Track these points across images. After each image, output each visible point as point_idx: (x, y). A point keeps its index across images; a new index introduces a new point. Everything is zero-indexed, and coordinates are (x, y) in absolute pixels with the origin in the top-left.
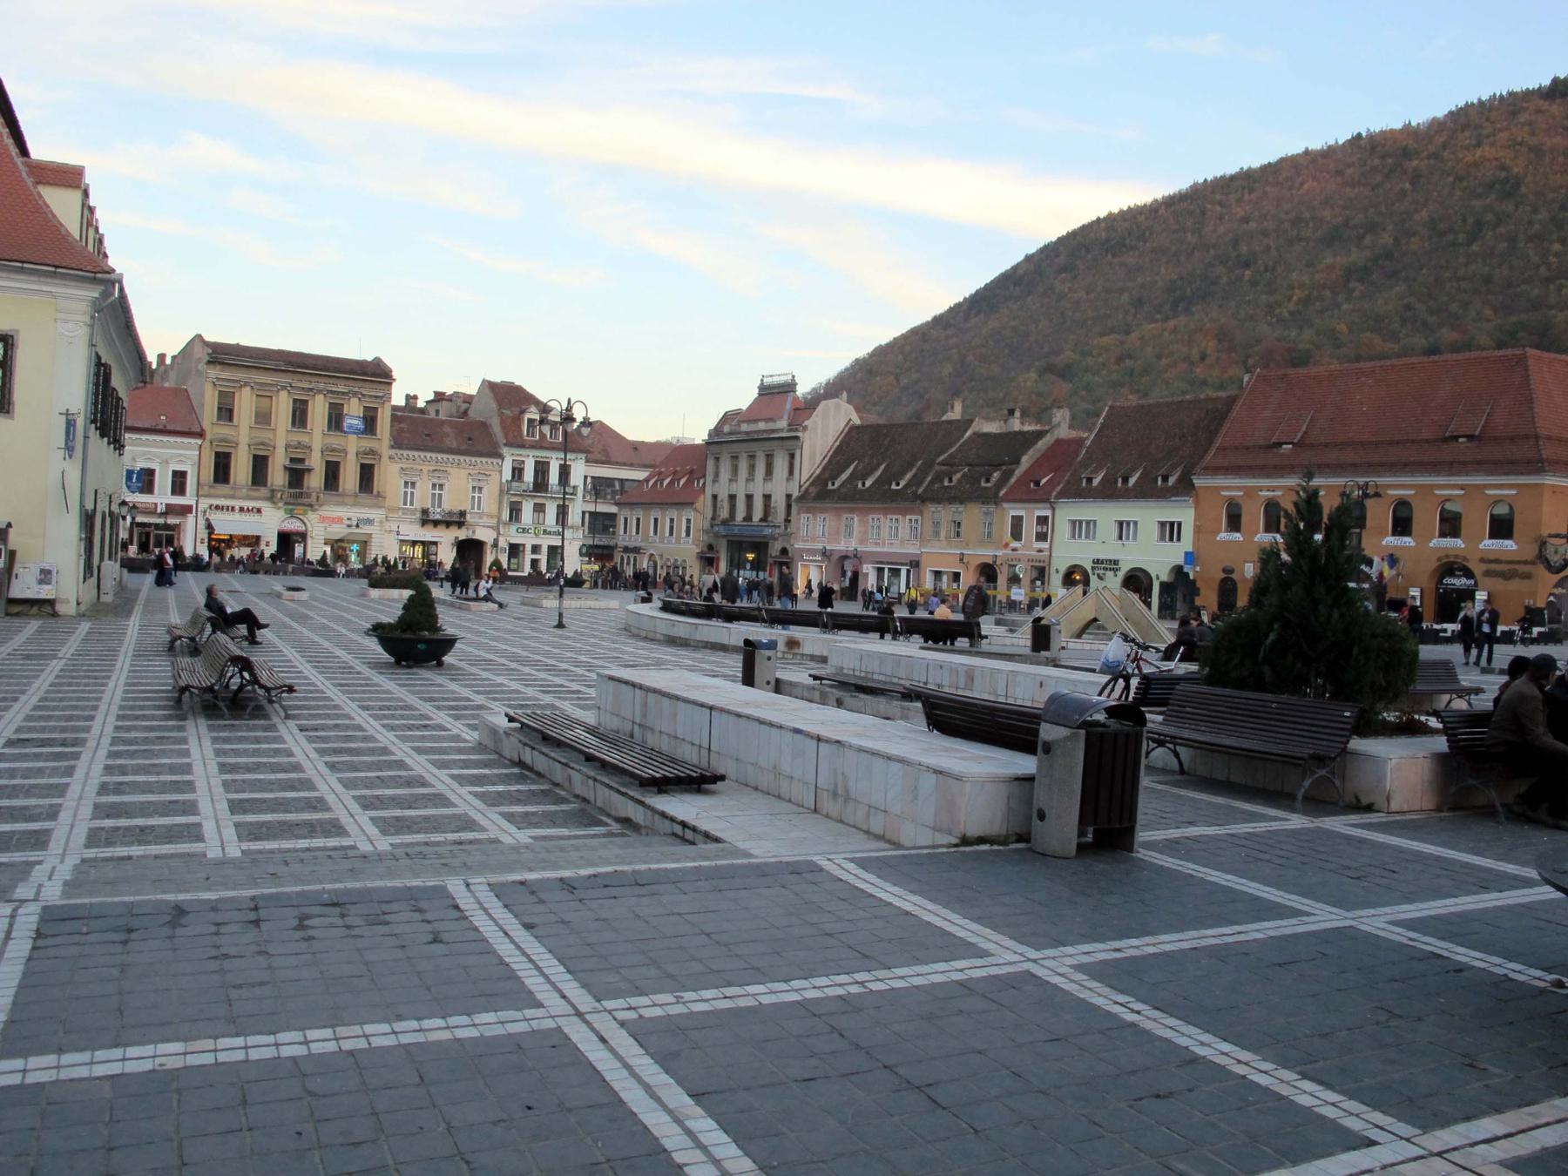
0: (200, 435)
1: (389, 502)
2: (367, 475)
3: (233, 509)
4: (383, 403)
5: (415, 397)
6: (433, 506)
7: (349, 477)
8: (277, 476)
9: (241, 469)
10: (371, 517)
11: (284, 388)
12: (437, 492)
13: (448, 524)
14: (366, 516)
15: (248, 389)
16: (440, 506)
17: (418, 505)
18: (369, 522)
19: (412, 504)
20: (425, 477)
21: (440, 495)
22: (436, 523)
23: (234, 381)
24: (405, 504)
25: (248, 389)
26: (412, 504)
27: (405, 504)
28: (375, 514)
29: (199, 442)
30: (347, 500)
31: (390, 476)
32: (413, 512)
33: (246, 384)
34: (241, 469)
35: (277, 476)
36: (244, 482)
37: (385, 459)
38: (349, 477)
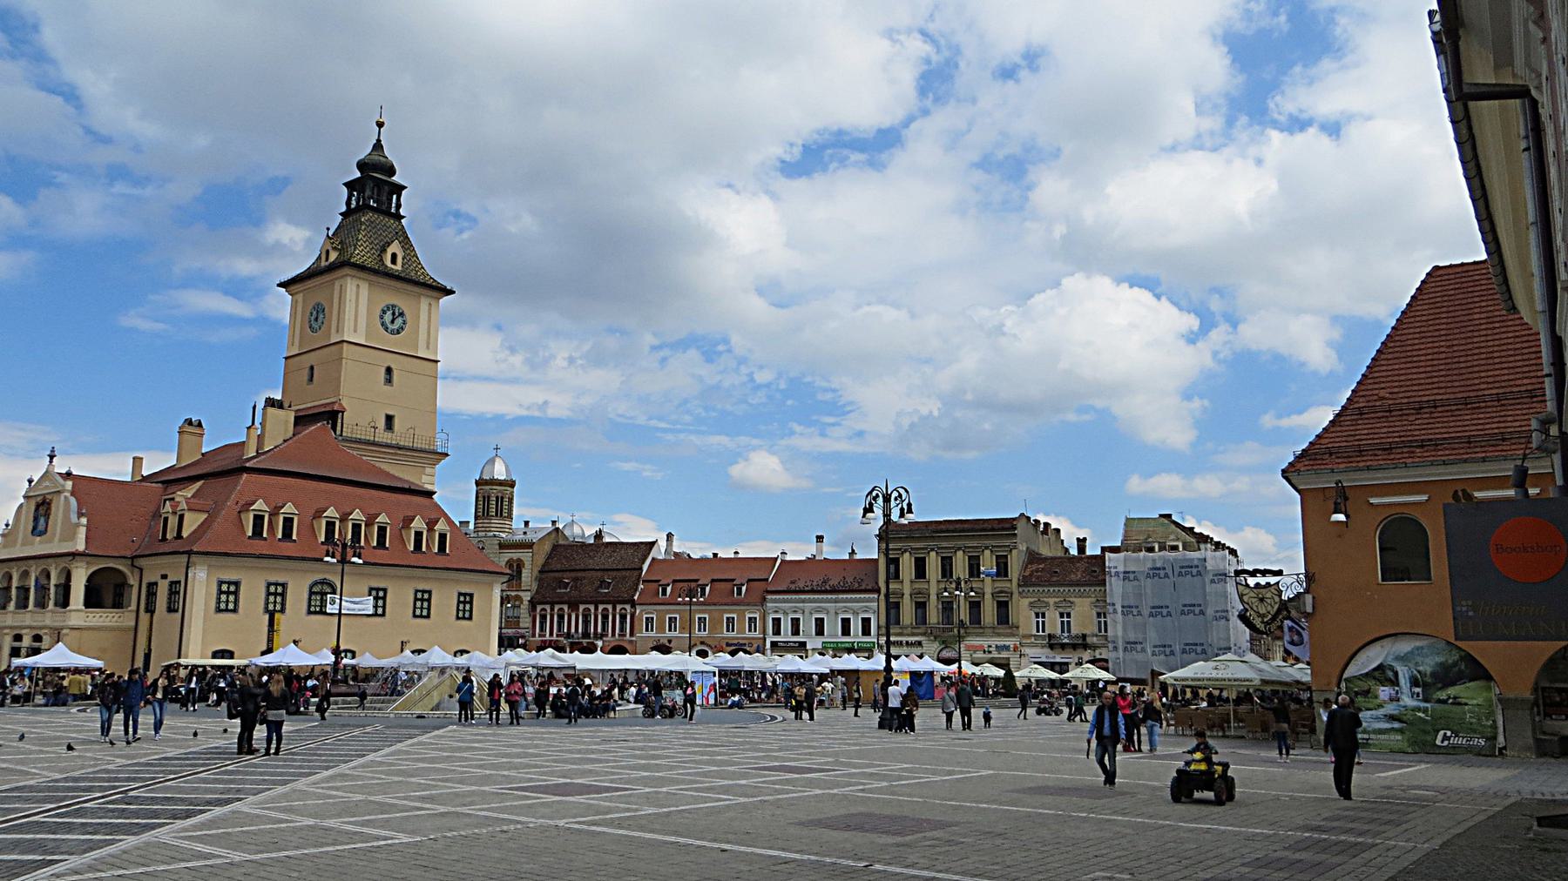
0: (878, 591)
1: (1021, 631)
2: (1003, 607)
3: (901, 642)
4: (1011, 551)
5: (1085, 539)
6: (1063, 631)
7: (989, 612)
8: (933, 616)
9: (907, 613)
10: (1007, 644)
11: (932, 550)
12: (1065, 619)
13: (1074, 647)
14: (1002, 643)
15: (908, 554)
16: (1069, 631)
17: (1047, 632)
18: (1006, 648)
19: (1043, 631)
20: (1052, 608)
21: (1069, 622)
22: (1063, 646)
23: (950, 548)
24: (1038, 631)
25: (908, 554)
26: (1043, 631)
27: (1038, 631)
28: (1010, 642)
29: (876, 596)
30: (986, 630)
31: (1022, 611)
32: (1043, 638)
33: (906, 551)
34: (907, 613)
35: (933, 616)
36: (909, 623)
37: (1016, 596)
38: (989, 612)
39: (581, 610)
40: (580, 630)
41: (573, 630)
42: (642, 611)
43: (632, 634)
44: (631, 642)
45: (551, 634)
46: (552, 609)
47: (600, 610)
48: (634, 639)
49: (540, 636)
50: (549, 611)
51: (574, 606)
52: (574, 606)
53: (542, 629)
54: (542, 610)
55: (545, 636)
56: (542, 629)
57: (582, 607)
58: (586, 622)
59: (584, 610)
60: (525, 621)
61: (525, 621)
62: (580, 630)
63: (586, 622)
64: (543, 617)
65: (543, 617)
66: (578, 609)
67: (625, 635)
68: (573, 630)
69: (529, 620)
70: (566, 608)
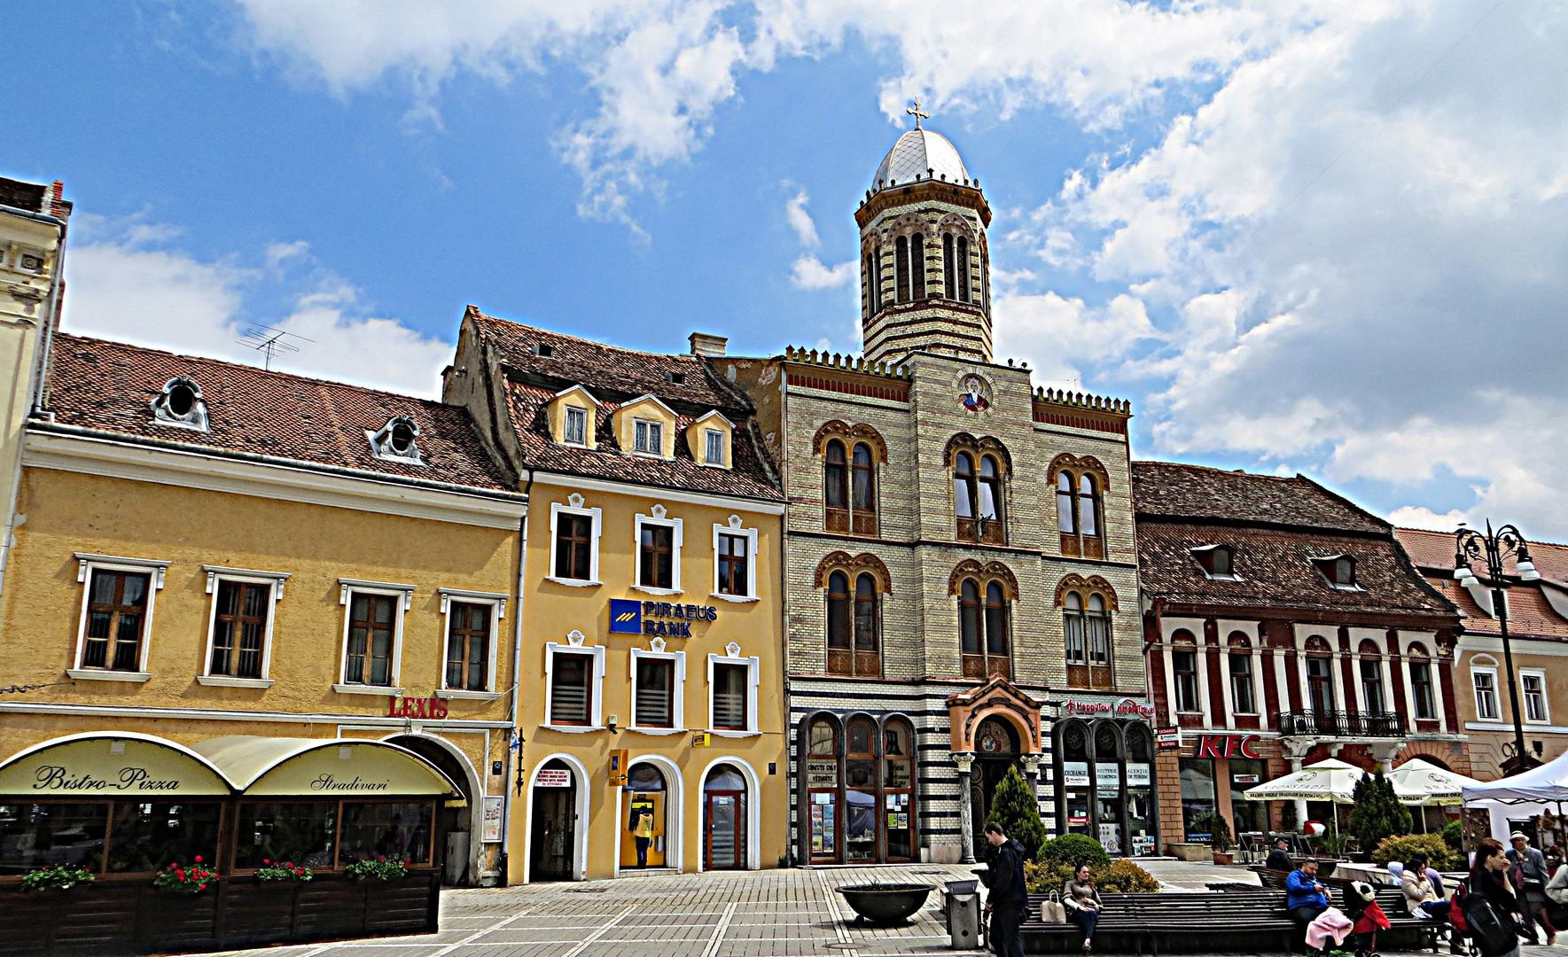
39: (1300, 644)
40: (1307, 704)
41: (1285, 707)
42: (1467, 654)
43: (1453, 725)
44: (1457, 745)
45: (1219, 718)
46: (1211, 635)
47: (1354, 647)
48: (1462, 737)
49: (1183, 722)
50: (1201, 638)
51: (1277, 629)
52: (1277, 629)
53: (1189, 700)
54: (1235, 636)
55: (1198, 722)
56: (1189, 700)
57: (1302, 632)
58: (1320, 682)
59: (1310, 643)
60: (1132, 672)
61: (1132, 672)
62: (1307, 704)
63: (1320, 682)
64: (1183, 661)
65: (1183, 661)
66: (1290, 641)
67: (1435, 726)
68: (1285, 707)
69: (1143, 665)
70: (1251, 629)
